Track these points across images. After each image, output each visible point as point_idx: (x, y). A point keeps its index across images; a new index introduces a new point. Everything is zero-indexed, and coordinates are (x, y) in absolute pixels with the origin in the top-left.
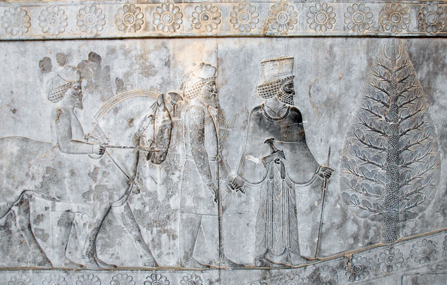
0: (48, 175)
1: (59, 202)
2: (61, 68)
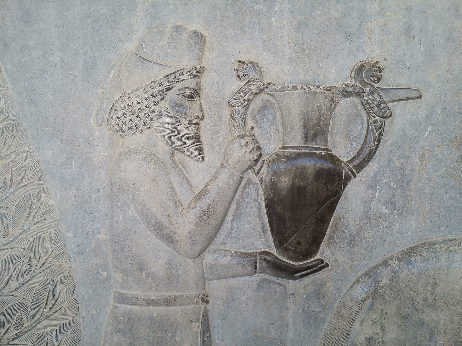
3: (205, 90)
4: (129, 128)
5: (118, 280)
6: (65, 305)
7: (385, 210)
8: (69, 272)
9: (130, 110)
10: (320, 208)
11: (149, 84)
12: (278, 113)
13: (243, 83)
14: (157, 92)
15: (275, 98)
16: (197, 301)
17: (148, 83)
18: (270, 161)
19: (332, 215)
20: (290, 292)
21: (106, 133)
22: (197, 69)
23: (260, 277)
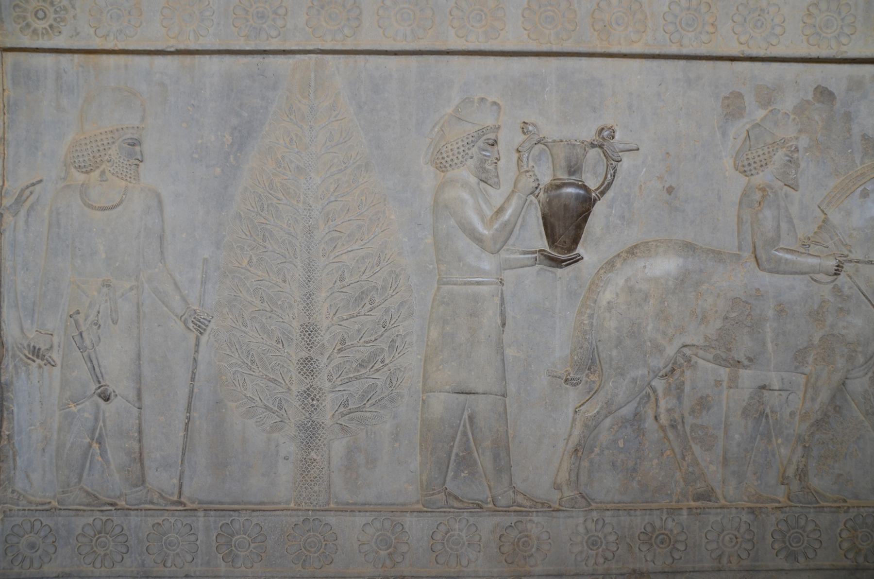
0: (734, 315)
1: (746, 369)
2: (761, 113)
3: (500, 142)
6: (403, 288)
7: (618, 222)
12: (550, 157)
20: (558, 277)
21: (432, 169)
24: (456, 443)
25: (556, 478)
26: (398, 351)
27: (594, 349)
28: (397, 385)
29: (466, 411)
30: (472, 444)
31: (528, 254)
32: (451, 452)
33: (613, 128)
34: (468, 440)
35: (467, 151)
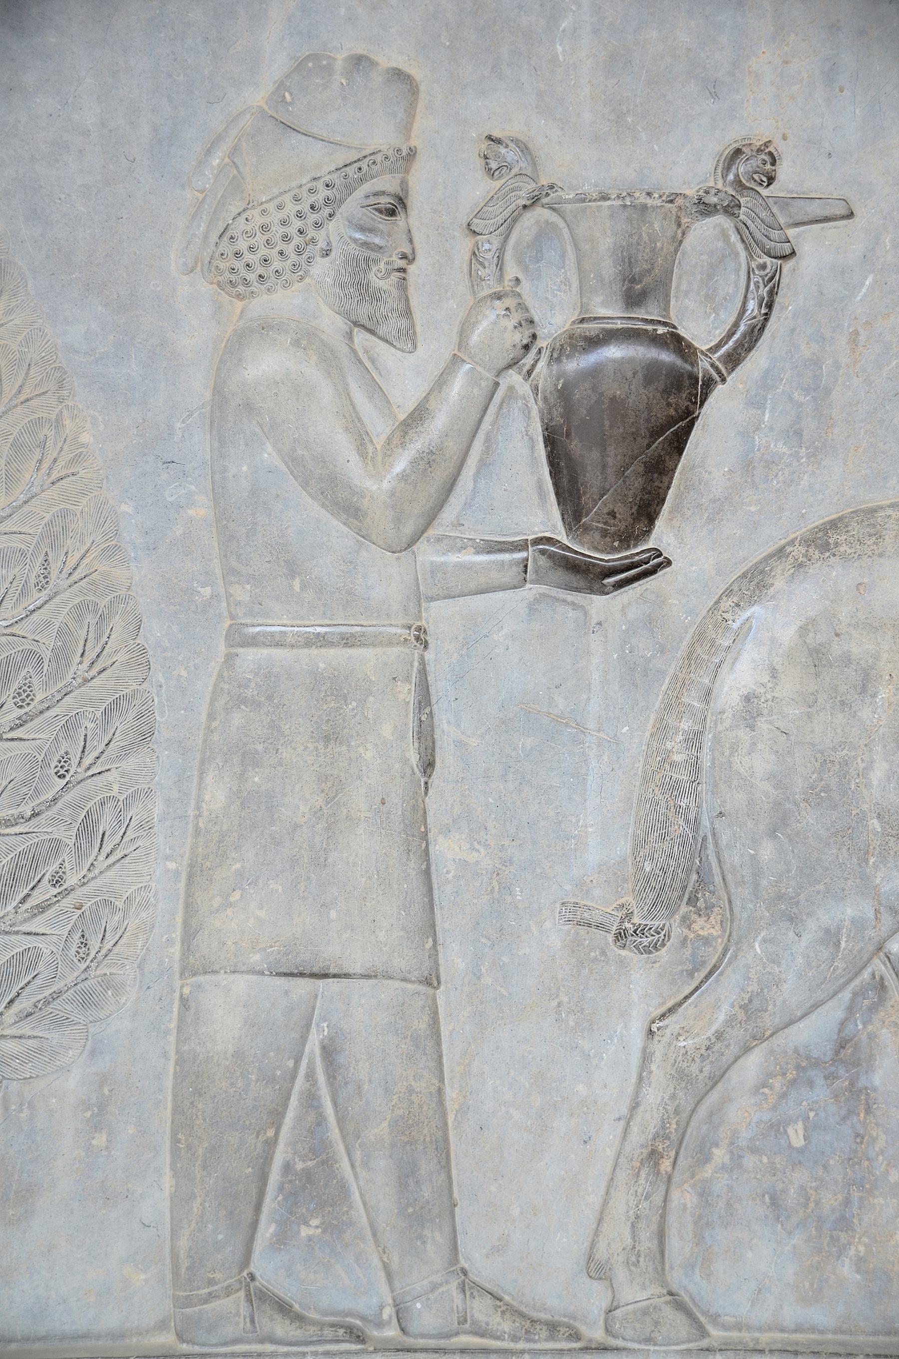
4: (260, 276)
5: (239, 598)
6: (122, 657)
7: (782, 448)
8: (129, 588)
9: (265, 238)
10: (654, 443)
11: (305, 184)
13: (497, 184)
14: (322, 201)
15: (563, 218)
16: (406, 640)
17: (304, 181)
18: (554, 349)
19: (679, 461)
20: (594, 621)
21: (205, 288)
22: (404, 154)
23: (534, 592)
24: (285, 1130)
25: (593, 1244)
26: (107, 848)
27: (705, 839)
28: (104, 952)
29: (313, 1030)
30: (334, 1133)
31: (501, 551)
32: (267, 1159)
33: (771, 149)
34: (321, 1120)
35: (311, 233)
